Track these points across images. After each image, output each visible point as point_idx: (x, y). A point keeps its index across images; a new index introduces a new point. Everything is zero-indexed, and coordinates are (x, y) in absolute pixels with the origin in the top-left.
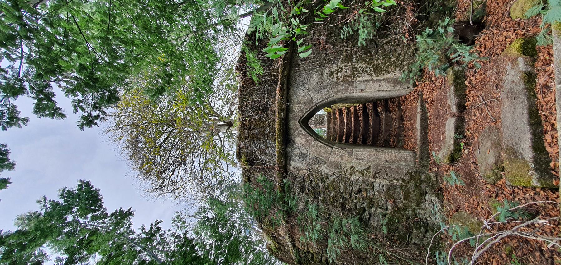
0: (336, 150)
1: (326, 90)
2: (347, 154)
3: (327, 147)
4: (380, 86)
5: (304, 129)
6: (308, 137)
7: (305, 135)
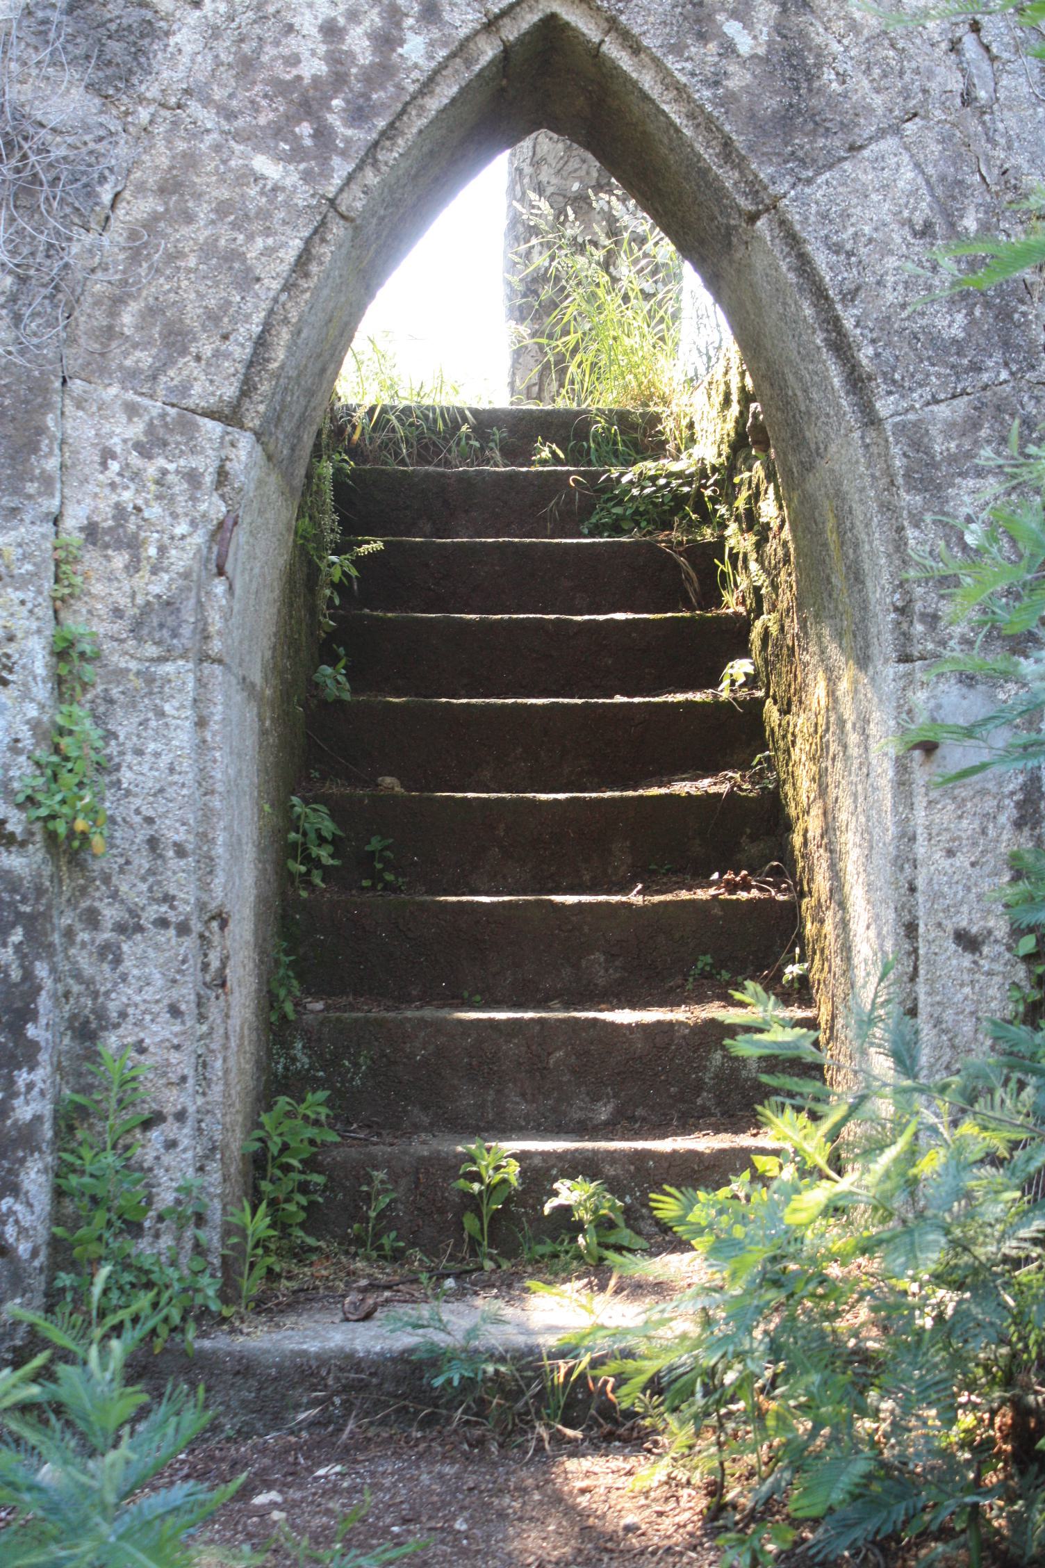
0: (206, 465)
1: (953, 325)
2: (158, 587)
3: (240, 350)
4: (968, 942)
5: (462, 50)
6: (358, 114)
7: (383, 71)
